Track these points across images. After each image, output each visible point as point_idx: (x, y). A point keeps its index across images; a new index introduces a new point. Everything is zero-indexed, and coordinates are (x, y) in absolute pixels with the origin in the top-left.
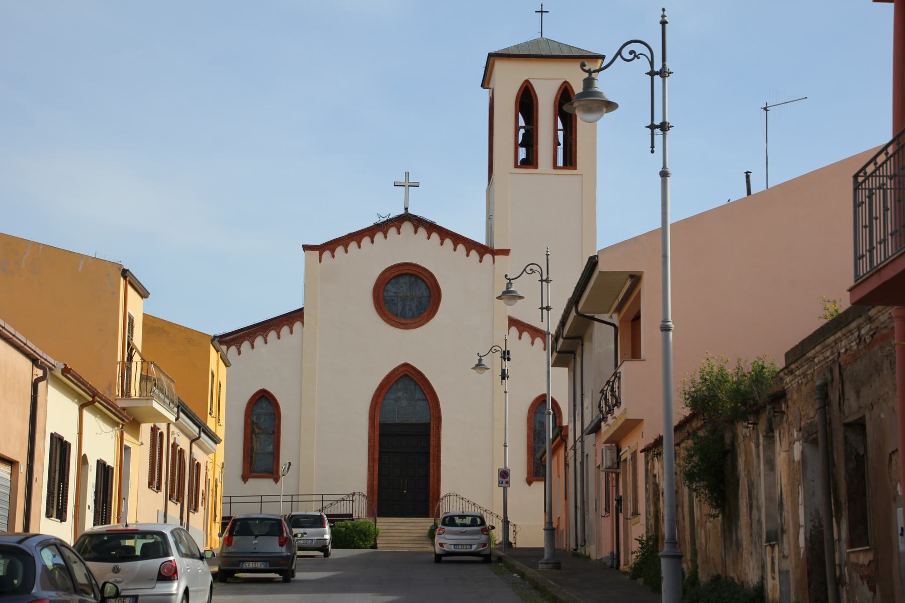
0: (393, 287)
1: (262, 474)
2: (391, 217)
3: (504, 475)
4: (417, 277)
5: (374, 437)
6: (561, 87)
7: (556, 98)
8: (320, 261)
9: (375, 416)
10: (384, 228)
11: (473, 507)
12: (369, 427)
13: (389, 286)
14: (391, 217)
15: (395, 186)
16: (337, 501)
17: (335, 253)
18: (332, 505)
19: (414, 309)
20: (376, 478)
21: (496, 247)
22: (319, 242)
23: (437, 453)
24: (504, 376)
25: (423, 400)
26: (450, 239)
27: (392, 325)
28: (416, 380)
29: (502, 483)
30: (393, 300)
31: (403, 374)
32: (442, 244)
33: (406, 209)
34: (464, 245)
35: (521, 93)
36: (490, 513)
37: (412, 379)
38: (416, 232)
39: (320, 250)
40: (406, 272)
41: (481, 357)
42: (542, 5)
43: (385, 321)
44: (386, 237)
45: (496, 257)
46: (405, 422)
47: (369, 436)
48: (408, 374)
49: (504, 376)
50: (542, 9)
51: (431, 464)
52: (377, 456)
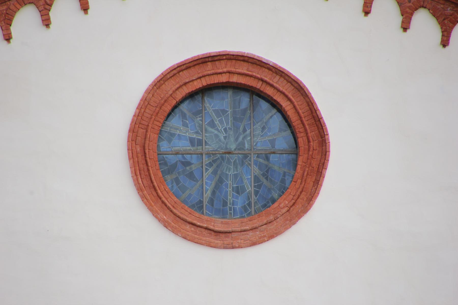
0: (185, 125)
19: (250, 188)
30: (187, 164)
40: (224, 79)
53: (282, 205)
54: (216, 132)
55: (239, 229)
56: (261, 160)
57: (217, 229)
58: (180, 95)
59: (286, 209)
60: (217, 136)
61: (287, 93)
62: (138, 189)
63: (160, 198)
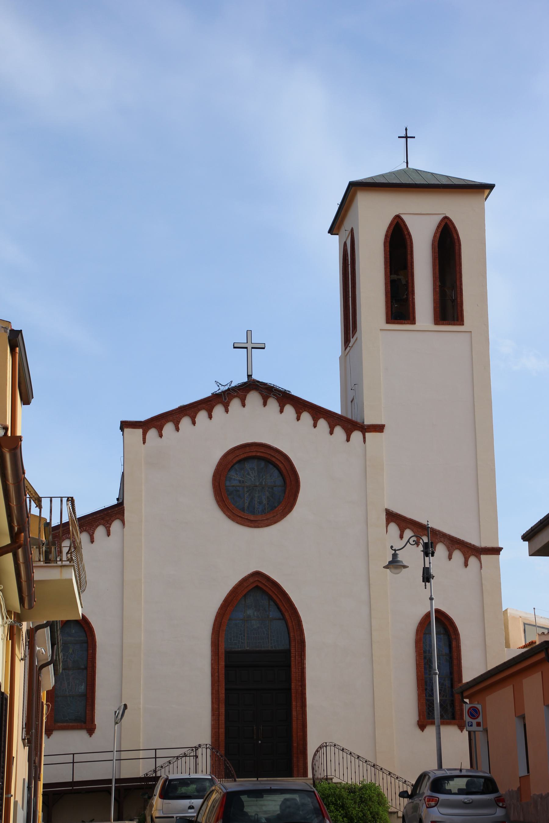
0: (237, 474)
1: (71, 724)
2: (233, 385)
3: (474, 713)
4: (268, 461)
5: (218, 669)
6: (440, 224)
7: (435, 236)
8: (144, 443)
9: (219, 641)
10: (225, 399)
11: (357, 760)
12: (212, 656)
13: (232, 473)
14: (233, 385)
15: (234, 348)
16: (177, 757)
17: (163, 432)
18: (170, 763)
19: (265, 502)
20: (223, 726)
21: (367, 422)
22: (143, 417)
23: (300, 688)
24: (427, 577)
25: (280, 619)
26: (309, 413)
27: (238, 523)
28: (270, 593)
29: (471, 726)
30: (238, 491)
31: (255, 585)
32: (298, 419)
33: (249, 376)
34: (326, 420)
35: (391, 231)
36: (379, 768)
37: (264, 592)
38: (265, 404)
39: (144, 427)
40: (254, 454)
41: (395, 550)
42: (406, 129)
43: (229, 517)
44: (227, 411)
45: (367, 435)
46: (258, 649)
47: (213, 668)
48: (260, 585)
49: (427, 577)
50: (406, 134)
51: (294, 703)
52: (222, 696)
53: (280, 509)
54: (250, 477)
55: (261, 519)
56: (270, 490)
57: (251, 519)
58: (235, 461)
59: (282, 511)
60: (250, 479)
61: (281, 460)
62: (217, 502)
63: (227, 506)
